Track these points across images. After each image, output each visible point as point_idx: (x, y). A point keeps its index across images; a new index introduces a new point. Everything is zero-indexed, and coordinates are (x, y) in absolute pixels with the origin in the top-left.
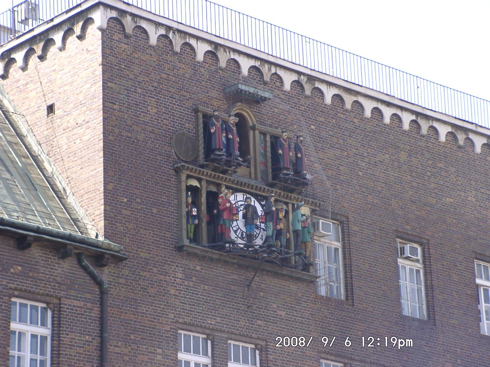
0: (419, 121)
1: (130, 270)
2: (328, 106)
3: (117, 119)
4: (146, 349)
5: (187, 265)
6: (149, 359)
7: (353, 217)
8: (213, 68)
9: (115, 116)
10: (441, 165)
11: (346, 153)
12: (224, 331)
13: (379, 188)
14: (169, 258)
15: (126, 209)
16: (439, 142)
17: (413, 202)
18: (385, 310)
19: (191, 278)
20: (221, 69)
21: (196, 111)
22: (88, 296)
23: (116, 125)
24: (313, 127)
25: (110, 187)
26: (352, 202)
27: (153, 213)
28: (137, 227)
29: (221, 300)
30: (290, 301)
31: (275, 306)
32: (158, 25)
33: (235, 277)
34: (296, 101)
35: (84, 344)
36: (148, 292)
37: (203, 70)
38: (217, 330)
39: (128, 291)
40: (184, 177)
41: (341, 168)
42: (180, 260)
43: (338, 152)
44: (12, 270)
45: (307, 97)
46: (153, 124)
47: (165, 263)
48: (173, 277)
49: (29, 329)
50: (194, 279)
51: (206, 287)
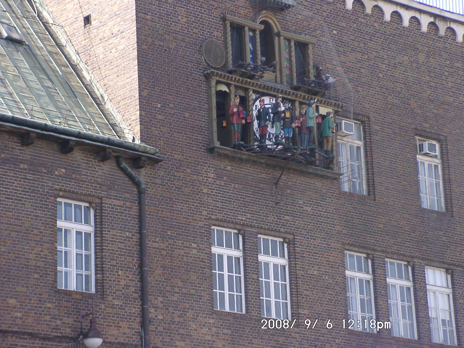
0: (437, 23)
1: (166, 171)
2: (349, 11)
3: (150, 29)
4: (182, 243)
5: (218, 166)
6: (184, 253)
7: (374, 117)
9: (147, 26)
11: (366, 56)
12: (254, 226)
13: (399, 89)
14: (201, 159)
15: (160, 114)
16: (456, 43)
18: (405, 203)
19: (223, 178)
21: (224, 19)
22: (128, 196)
23: (149, 34)
24: (335, 32)
25: (145, 93)
26: (373, 102)
27: (185, 117)
28: (171, 131)
29: (251, 197)
30: (315, 197)
31: (301, 202)
33: (263, 176)
34: (318, 7)
35: (125, 240)
36: (182, 192)
38: (247, 225)
39: (164, 191)
40: (213, 83)
41: (362, 70)
42: (212, 161)
43: (359, 56)
44: (56, 173)
46: (183, 33)
47: (197, 164)
48: (205, 177)
49: (74, 227)
50: (225, 178)
51: (236, 186)
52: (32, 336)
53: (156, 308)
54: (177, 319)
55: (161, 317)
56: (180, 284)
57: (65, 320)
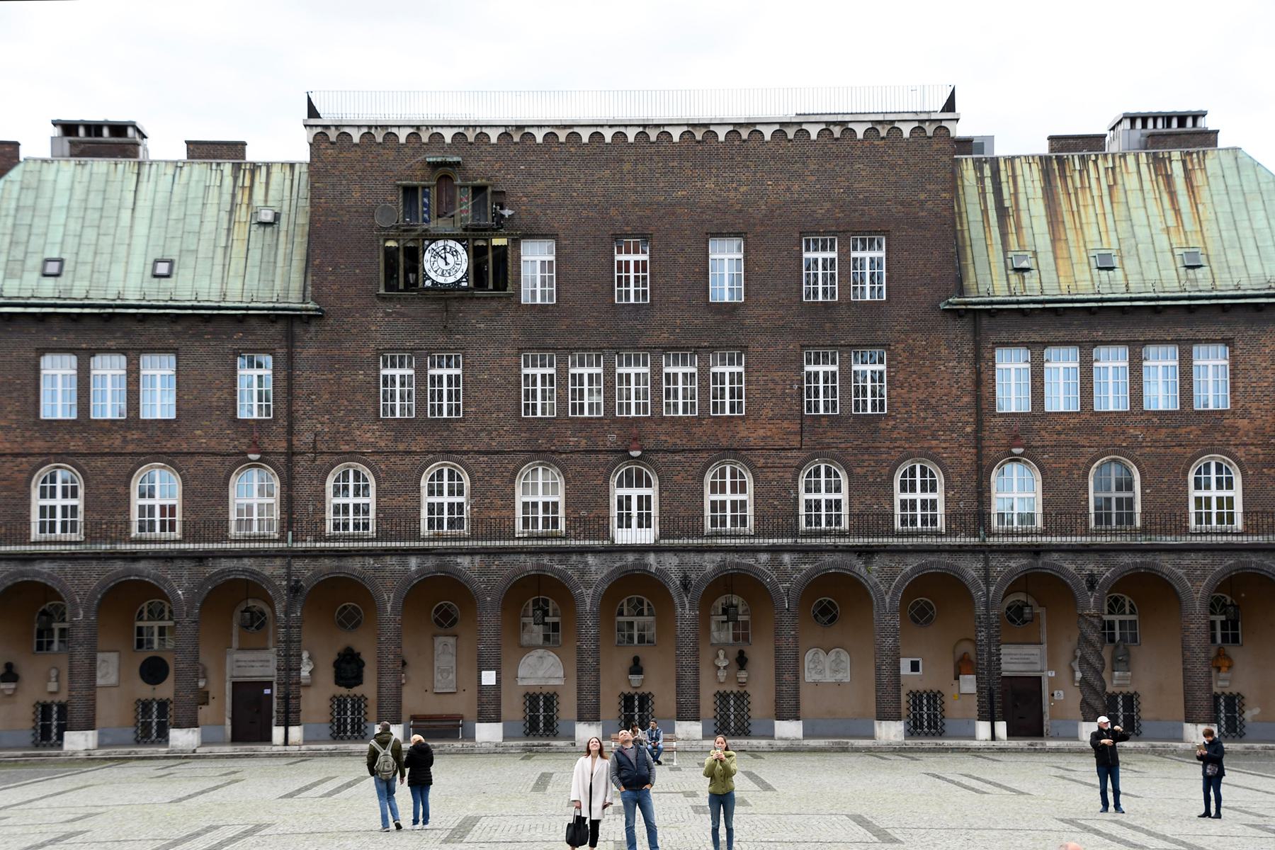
0: (647, 131)
8: (417, 145)
10: (675, 164)
13: (596, 202)
17: (637, 205)
20: (424, 144)
32: (359, 127)
34: (504, 149)
37: (406, 150)
40: (381, 242)
43: (550, 182)
45: (516, 143)
52: (213, 454)
53: (323, 423)
54: (342, 430)
55: (326, 430)
56: (346, 403)
57: (242, 440)
